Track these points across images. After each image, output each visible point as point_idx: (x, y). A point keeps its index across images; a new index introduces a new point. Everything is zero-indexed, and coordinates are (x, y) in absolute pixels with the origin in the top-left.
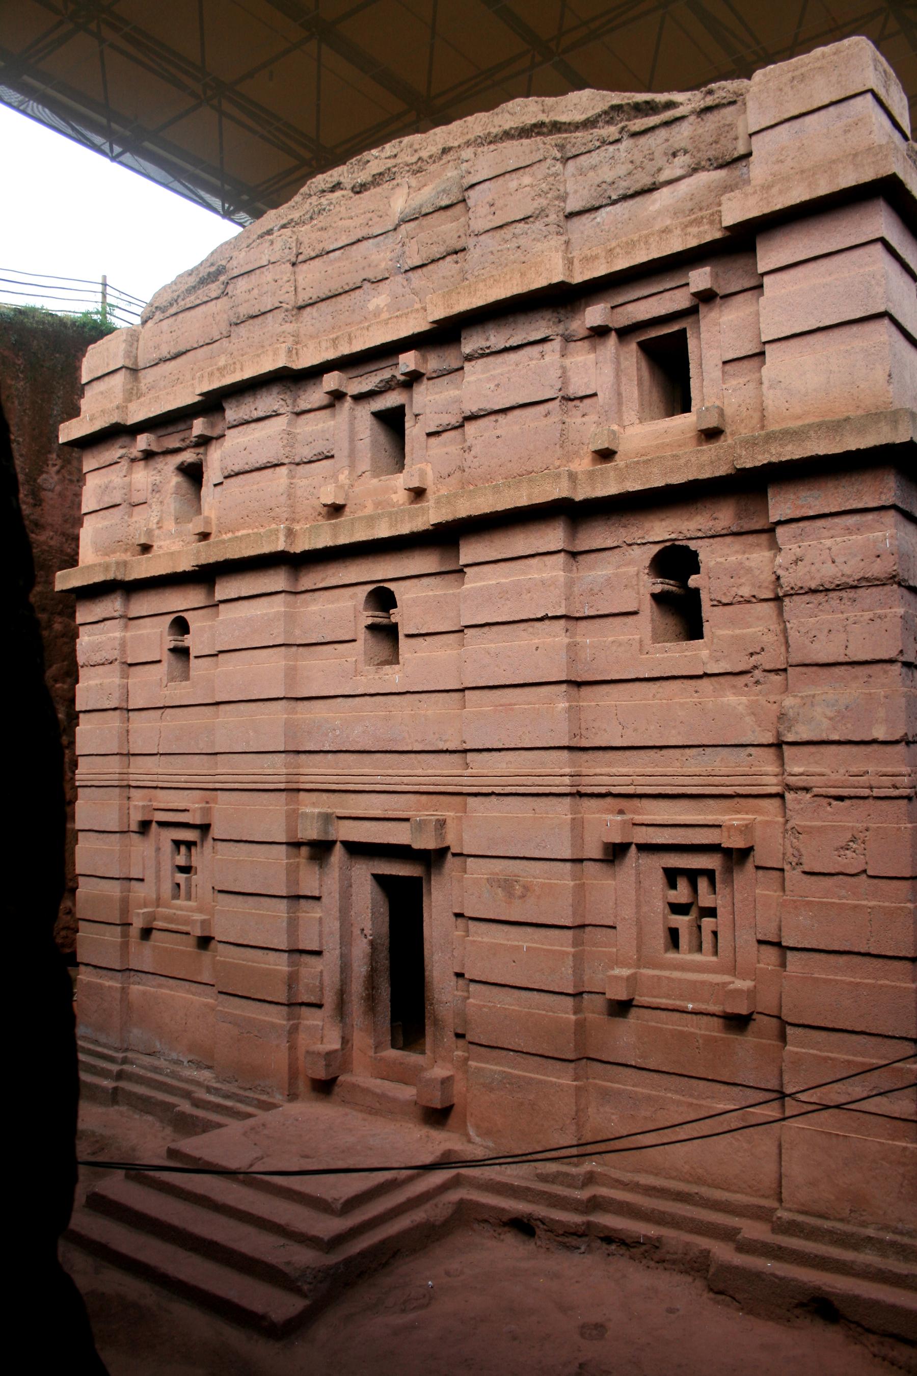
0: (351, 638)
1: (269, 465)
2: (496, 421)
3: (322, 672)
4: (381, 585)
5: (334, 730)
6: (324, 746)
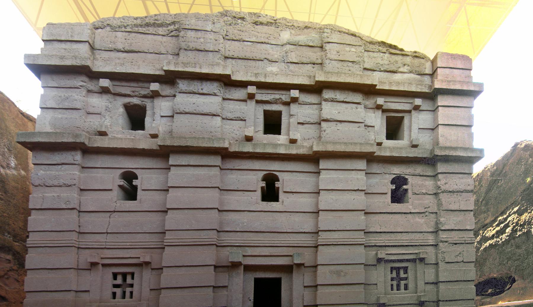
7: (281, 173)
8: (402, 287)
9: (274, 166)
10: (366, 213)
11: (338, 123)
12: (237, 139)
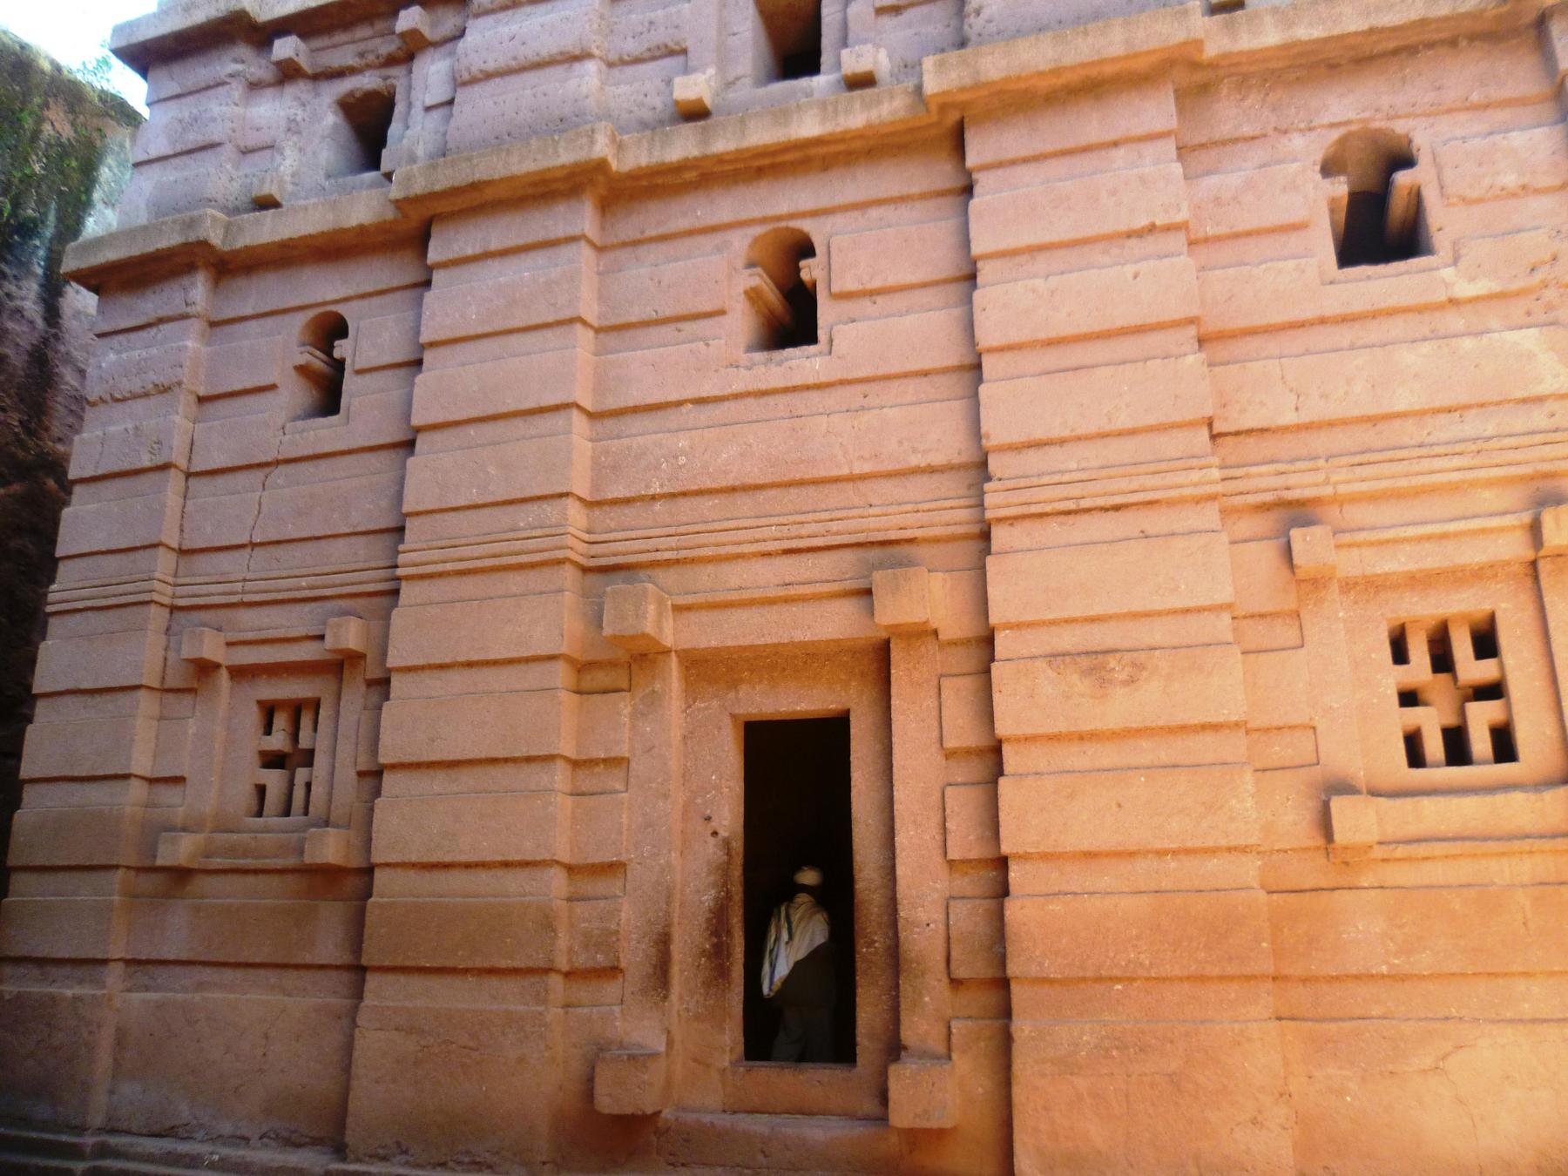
3: (649, 370)
4: (783, 224)
5: (676, 457)
6: (647, 486)
8: (1480, 743)
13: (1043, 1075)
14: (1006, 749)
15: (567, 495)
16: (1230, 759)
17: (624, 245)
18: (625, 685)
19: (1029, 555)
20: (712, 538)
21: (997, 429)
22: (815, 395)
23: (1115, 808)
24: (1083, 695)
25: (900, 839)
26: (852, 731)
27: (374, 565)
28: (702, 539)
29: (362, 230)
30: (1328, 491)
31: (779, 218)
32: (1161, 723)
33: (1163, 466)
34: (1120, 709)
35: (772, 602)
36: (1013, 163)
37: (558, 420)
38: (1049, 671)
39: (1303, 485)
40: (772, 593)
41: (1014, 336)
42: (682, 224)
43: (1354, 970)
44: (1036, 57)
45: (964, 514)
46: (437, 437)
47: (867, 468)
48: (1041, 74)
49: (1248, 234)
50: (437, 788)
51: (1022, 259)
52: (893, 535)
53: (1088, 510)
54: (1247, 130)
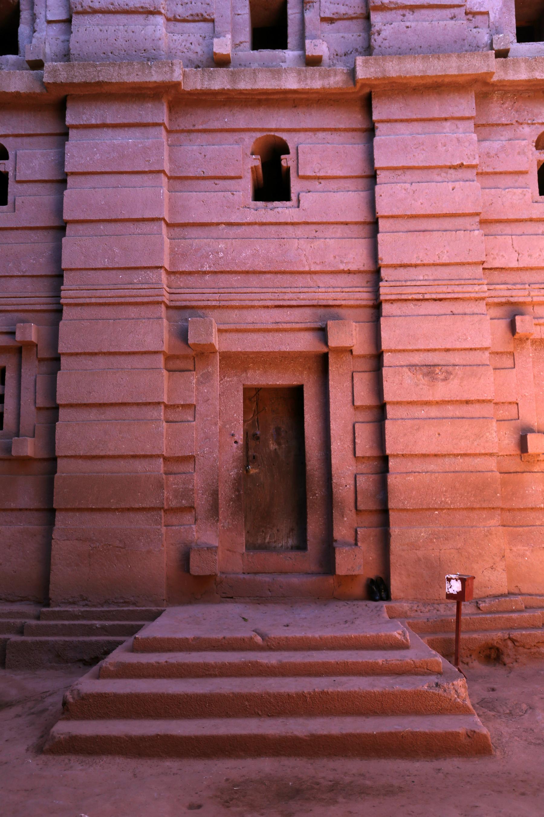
0: (236, 175)
1: (141, 10)
2: (404, 15)
3: (200, 204)
4: (272, 133)
5: (218, 253)
6: (202, 267)
7: (293, 134)
9: (277, 121)
10: (484, 222)
11: (407, 12)
12: (197, 63)
13: (403, 550)
14: (388, 408)
15: (161, 267)
16: (486, 416)
17: (183, 131)
18: (192, 368)
19: (401, 318)
20: (238, 296)
21: (385, 256)
22: (290, 228)
23: (437, 435)
24: (424, 385)
25: (334, 447)
26: (305, 395)
27: (38, 294)
28: (233, 296)
29: (17, 95)
30: (529, 299)
31: (270, 130)
32: (458, 399)
33: (463, 282)
34: (442, 391)
35: (268, 331)
36: (396, 121)
37: (154, 227)
38: (409, 373)
39: (519, 296)
40: (270, 326)
41: (396, 212)
42: (217, 125)
43: (530, 506)
44: (413, 68)
45: (365, 296)
46: (80, 227)
47: (318, 268)
48: (416, 77)
49: (501, 173)
50: (92, 417)
51: (399, 172)
52: (331, 303)
53: (427, 300)
54: (504, 120)
